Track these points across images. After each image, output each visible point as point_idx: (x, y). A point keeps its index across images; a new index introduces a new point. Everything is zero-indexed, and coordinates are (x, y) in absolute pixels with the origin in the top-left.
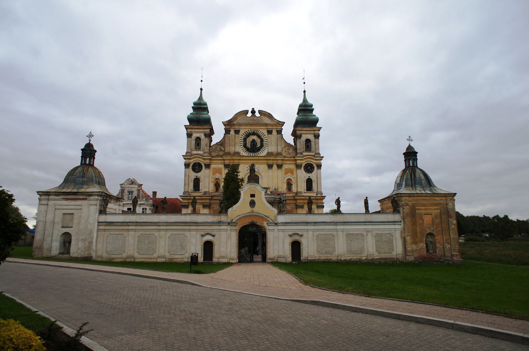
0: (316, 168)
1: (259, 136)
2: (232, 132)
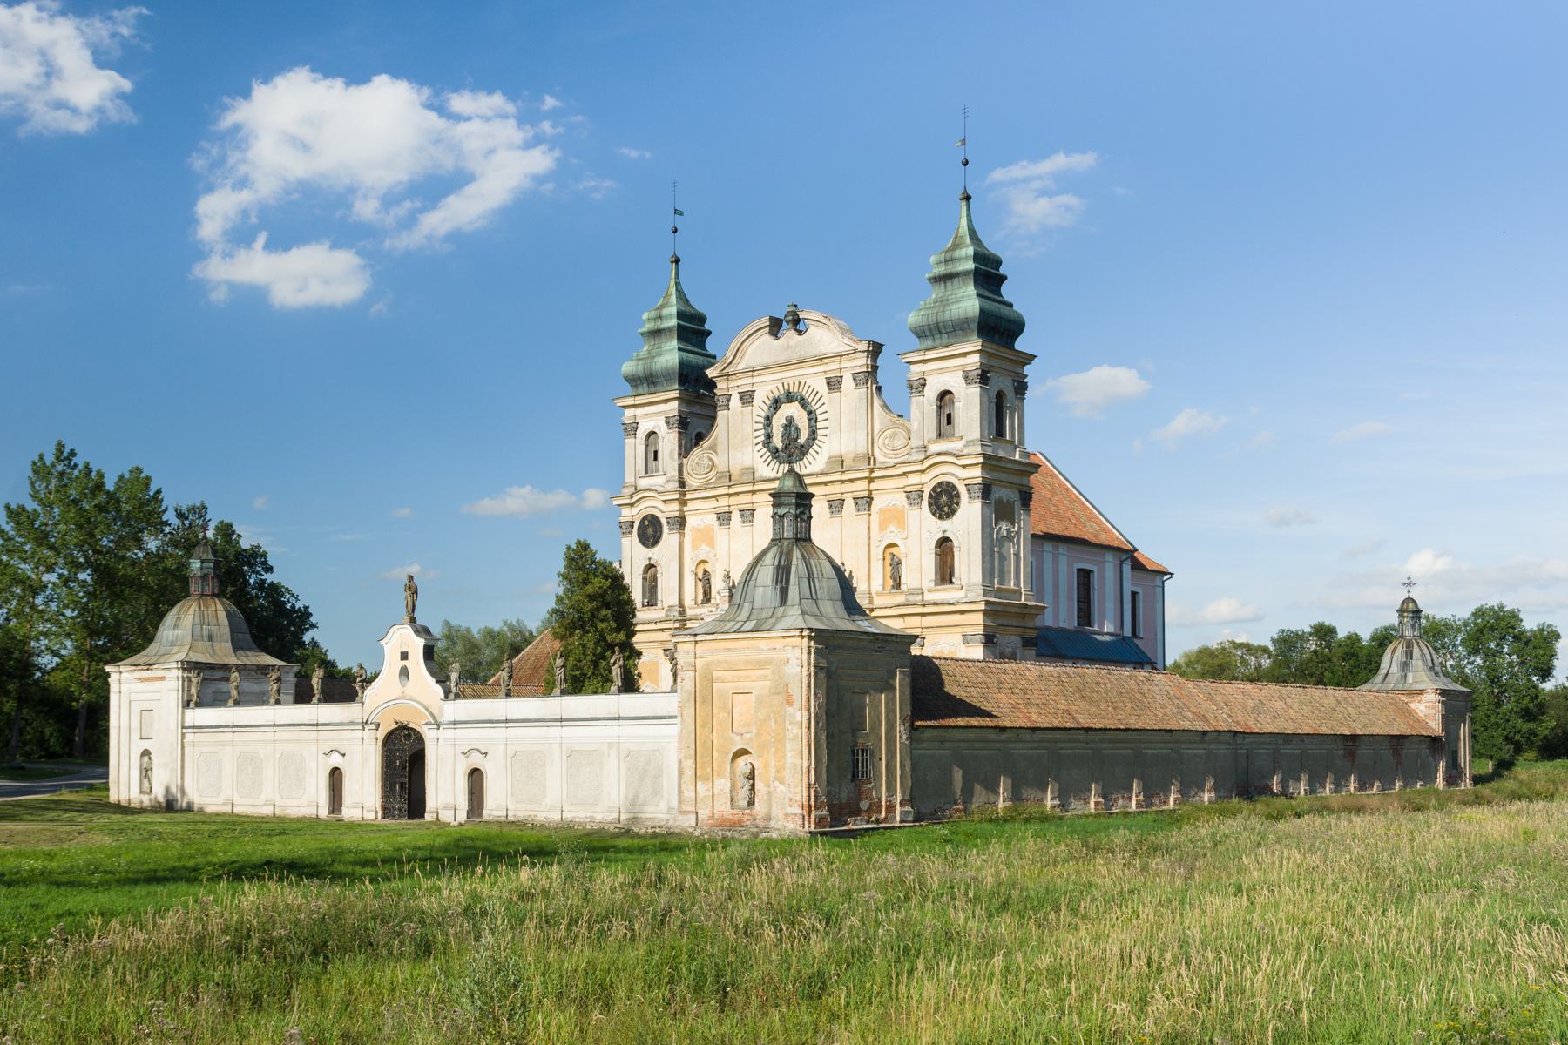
1: (803, 403)
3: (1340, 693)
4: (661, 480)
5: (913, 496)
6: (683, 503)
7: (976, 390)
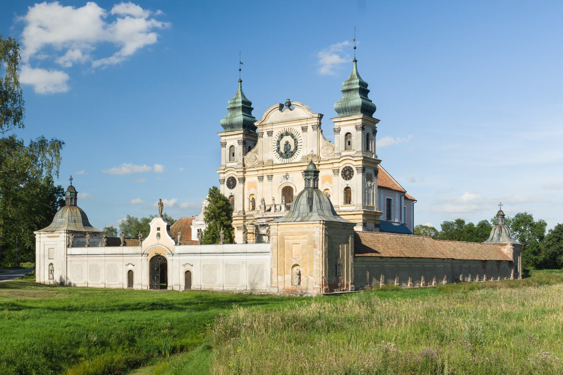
0: (355, 172)
1: (293, 136)
3: (477, 245)
4: (235, 164)
5: (336, 172)
6: (244, 172)
7: (360, 133)
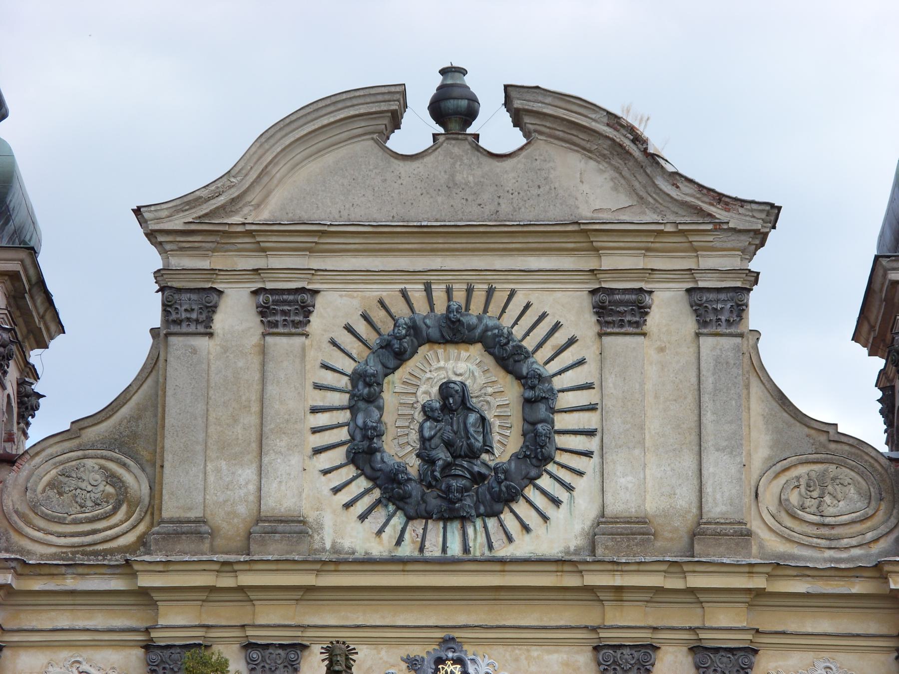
1: (507, 356)
2: (235, 314)
